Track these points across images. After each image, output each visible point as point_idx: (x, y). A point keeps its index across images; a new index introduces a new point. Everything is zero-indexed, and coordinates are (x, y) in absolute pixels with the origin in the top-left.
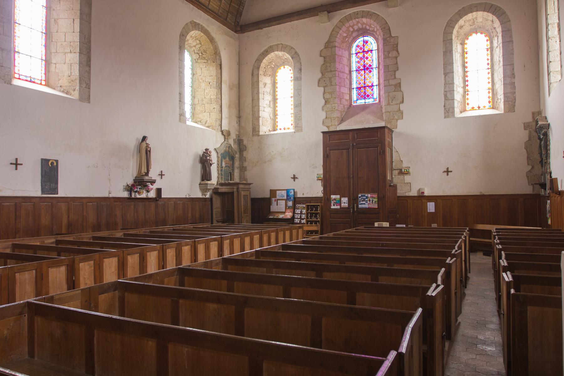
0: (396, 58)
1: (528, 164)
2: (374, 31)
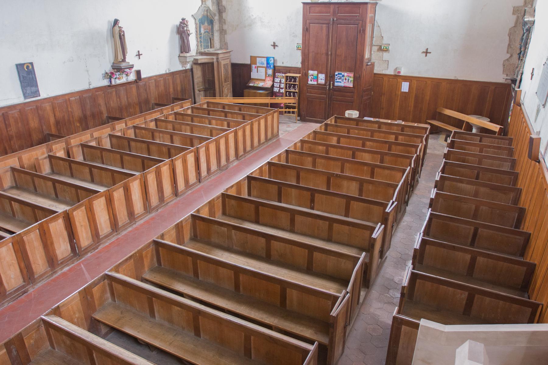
1: (508, 52)
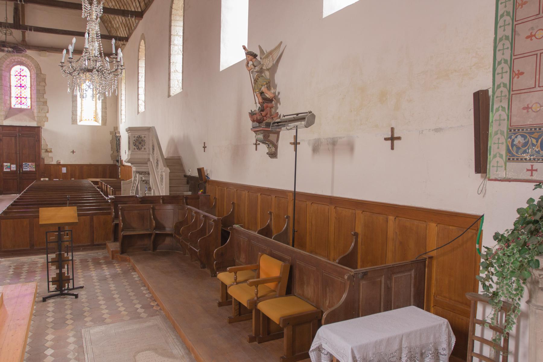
0: (44, 86)
1: (112, 151)
2: (29, 66)
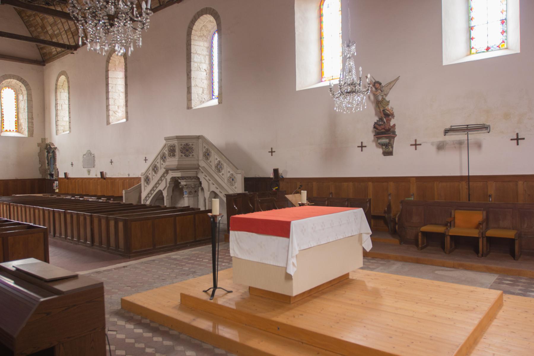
1: (40, 164)
